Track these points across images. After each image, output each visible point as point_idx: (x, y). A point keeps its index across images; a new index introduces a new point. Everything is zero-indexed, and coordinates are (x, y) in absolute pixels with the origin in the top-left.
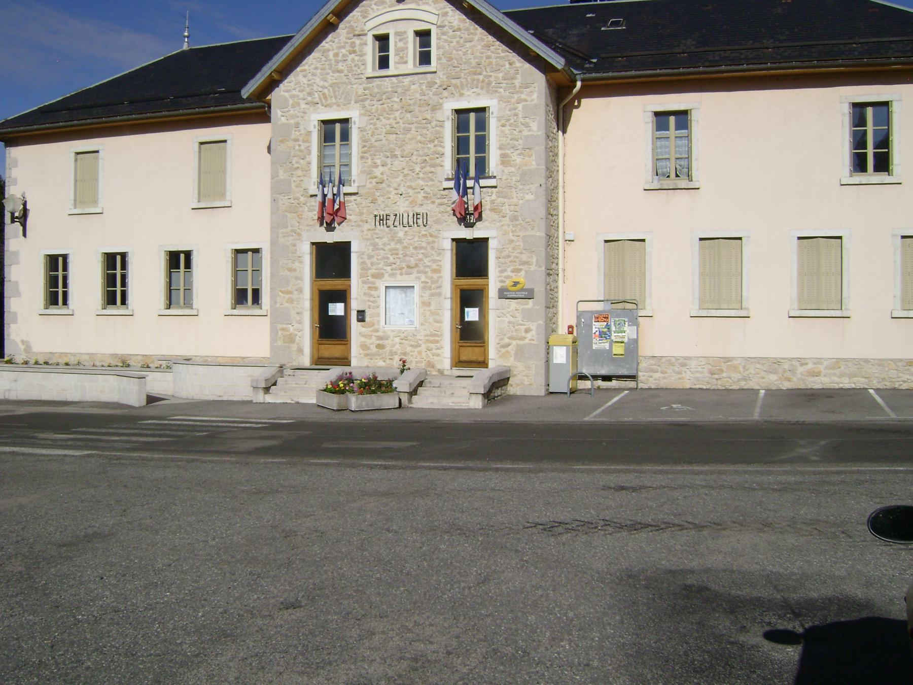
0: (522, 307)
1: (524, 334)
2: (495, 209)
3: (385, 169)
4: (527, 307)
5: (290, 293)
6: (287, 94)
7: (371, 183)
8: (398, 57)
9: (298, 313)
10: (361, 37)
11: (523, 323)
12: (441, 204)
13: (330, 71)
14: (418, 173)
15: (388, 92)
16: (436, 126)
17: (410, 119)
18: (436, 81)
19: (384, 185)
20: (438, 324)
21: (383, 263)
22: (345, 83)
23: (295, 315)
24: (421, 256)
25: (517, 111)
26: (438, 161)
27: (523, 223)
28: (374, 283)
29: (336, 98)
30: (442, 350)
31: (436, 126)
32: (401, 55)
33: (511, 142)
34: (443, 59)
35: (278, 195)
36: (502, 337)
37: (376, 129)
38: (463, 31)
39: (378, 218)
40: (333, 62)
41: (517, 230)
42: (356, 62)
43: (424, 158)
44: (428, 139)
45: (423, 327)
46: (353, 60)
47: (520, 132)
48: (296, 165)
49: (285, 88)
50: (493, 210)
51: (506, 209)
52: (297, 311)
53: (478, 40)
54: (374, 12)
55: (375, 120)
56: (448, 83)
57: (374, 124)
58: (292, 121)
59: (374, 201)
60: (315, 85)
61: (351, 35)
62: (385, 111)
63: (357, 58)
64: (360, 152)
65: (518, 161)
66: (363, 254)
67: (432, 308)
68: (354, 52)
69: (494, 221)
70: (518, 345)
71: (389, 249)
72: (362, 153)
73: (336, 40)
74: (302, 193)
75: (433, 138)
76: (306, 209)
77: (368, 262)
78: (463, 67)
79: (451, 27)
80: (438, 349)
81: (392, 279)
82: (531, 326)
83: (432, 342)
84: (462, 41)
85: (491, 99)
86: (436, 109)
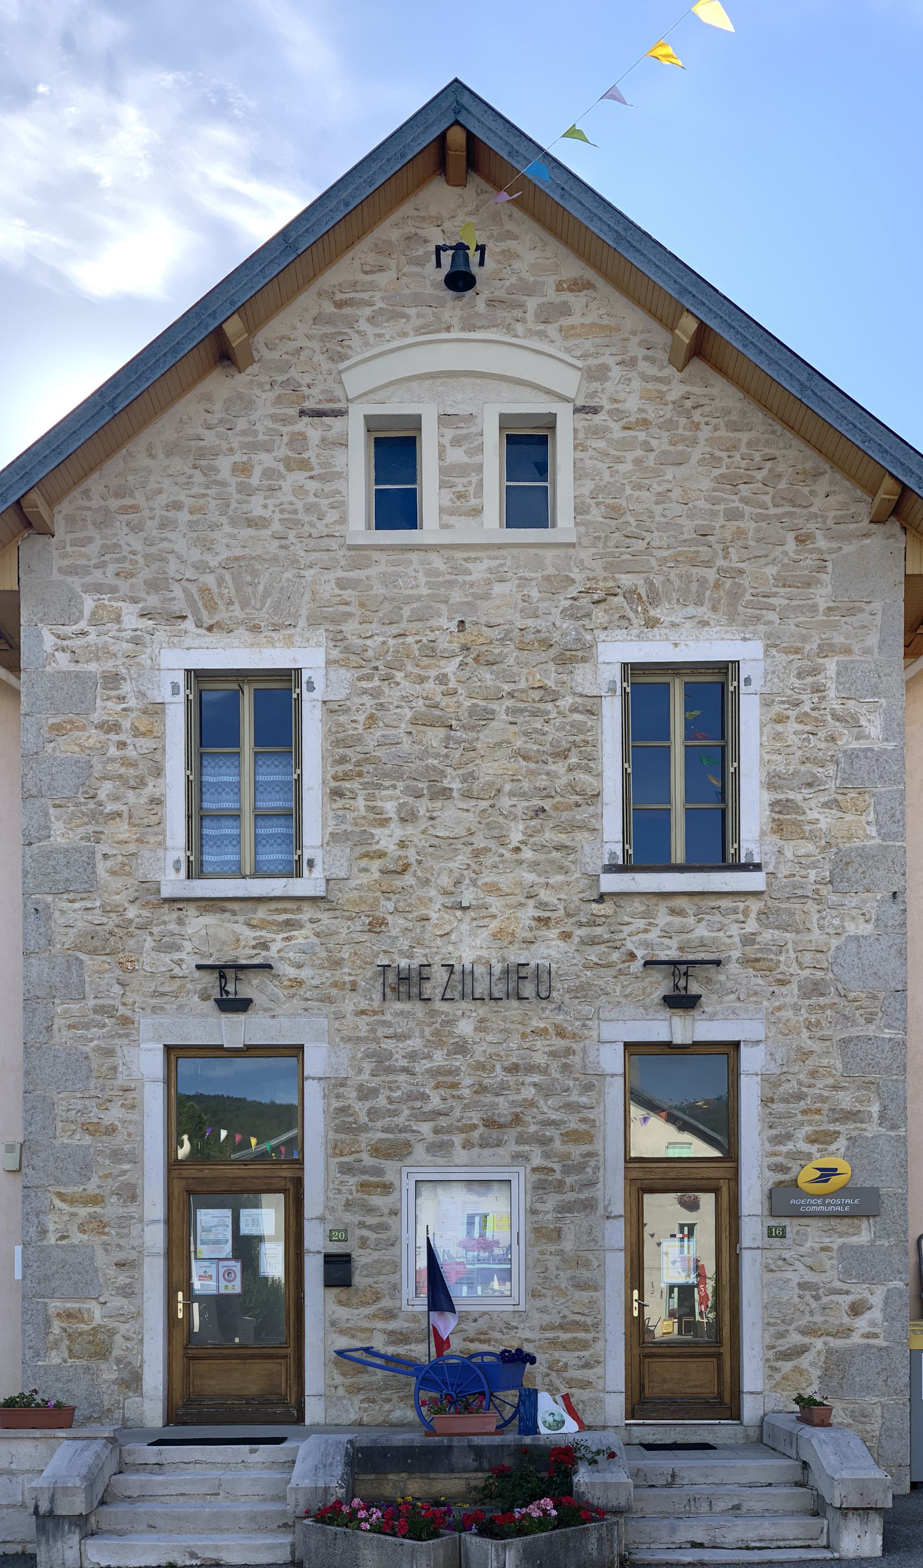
0: (840, 1241)
1: (846, 1320)
2: (757, 960)
3: (410, 829)
4: (854, 1240)
5: (96, 1200)
6: (75, 582)
7: (366, 870)
8: (448, 494)
9: (120, 1265)
10: (324, 419)
11: (845, 1287)
12: (593, 942)
13: (224, 520)
14: (517, 850)
15: (419, 598)
16: (574, 709)
17: (489, 683)
18: (572, 575)
19: (408, 879)
20: (584, 1293)
21: (406, 1112)
22: (275, 559)
23: (112, 1272)
24: (529, 1093)
25: (820, 678)
26: (581, 815)
27: (842, 1002)
28: (378, 1171)
29: (244, 605)
30: (598, 1370)
31: (574, 709)
32: (460, 488)
33: (803, 769)
34: (594, 511)
35: (49, 898)
36: (782, 1328)
37: (381, 707)
38: (654, 430)
39: (392, 978)
40: (232, 489)
41: (824, 1022)
42: (312, 499)
43: (537, 802)
44: (547, 748)
45: (539, 1303)
46: (299, 490)
47: (832, 739)
48: (109, 808)
49: (66, 562)
50: (746, 962)
51: (787, 963)
52: (120, 1256)
53: (701, 462)
54: (367, 344)
55: (376, 683)
56: (610, 584)
57: (376, 693)
58: (93, 667)
59: (377, 925)
60: (171, 558)
61: (293, 412)
62: (408, 657)
63: (312, 486)
64: (329, 777)
65: (823, 825)
66: (343, 1083)
67: (568, 1245)
68: (305, 465)
69: (756, 993)
70: (830, 1352)
71: (428, 1071)
72: (335, 778)
73: (242, 424)
74: (132, 895)
75: (565, 745)
76: (149, 943)
77: (361, 1109)
78: (657, 539)
79: (618, 414)
80: (587, 1366)
81: (440, 1161)
82: (866, 1294)
83: (564, 1346)
84: (651, 458)
85: (744, 639)
86: (573, 660)
